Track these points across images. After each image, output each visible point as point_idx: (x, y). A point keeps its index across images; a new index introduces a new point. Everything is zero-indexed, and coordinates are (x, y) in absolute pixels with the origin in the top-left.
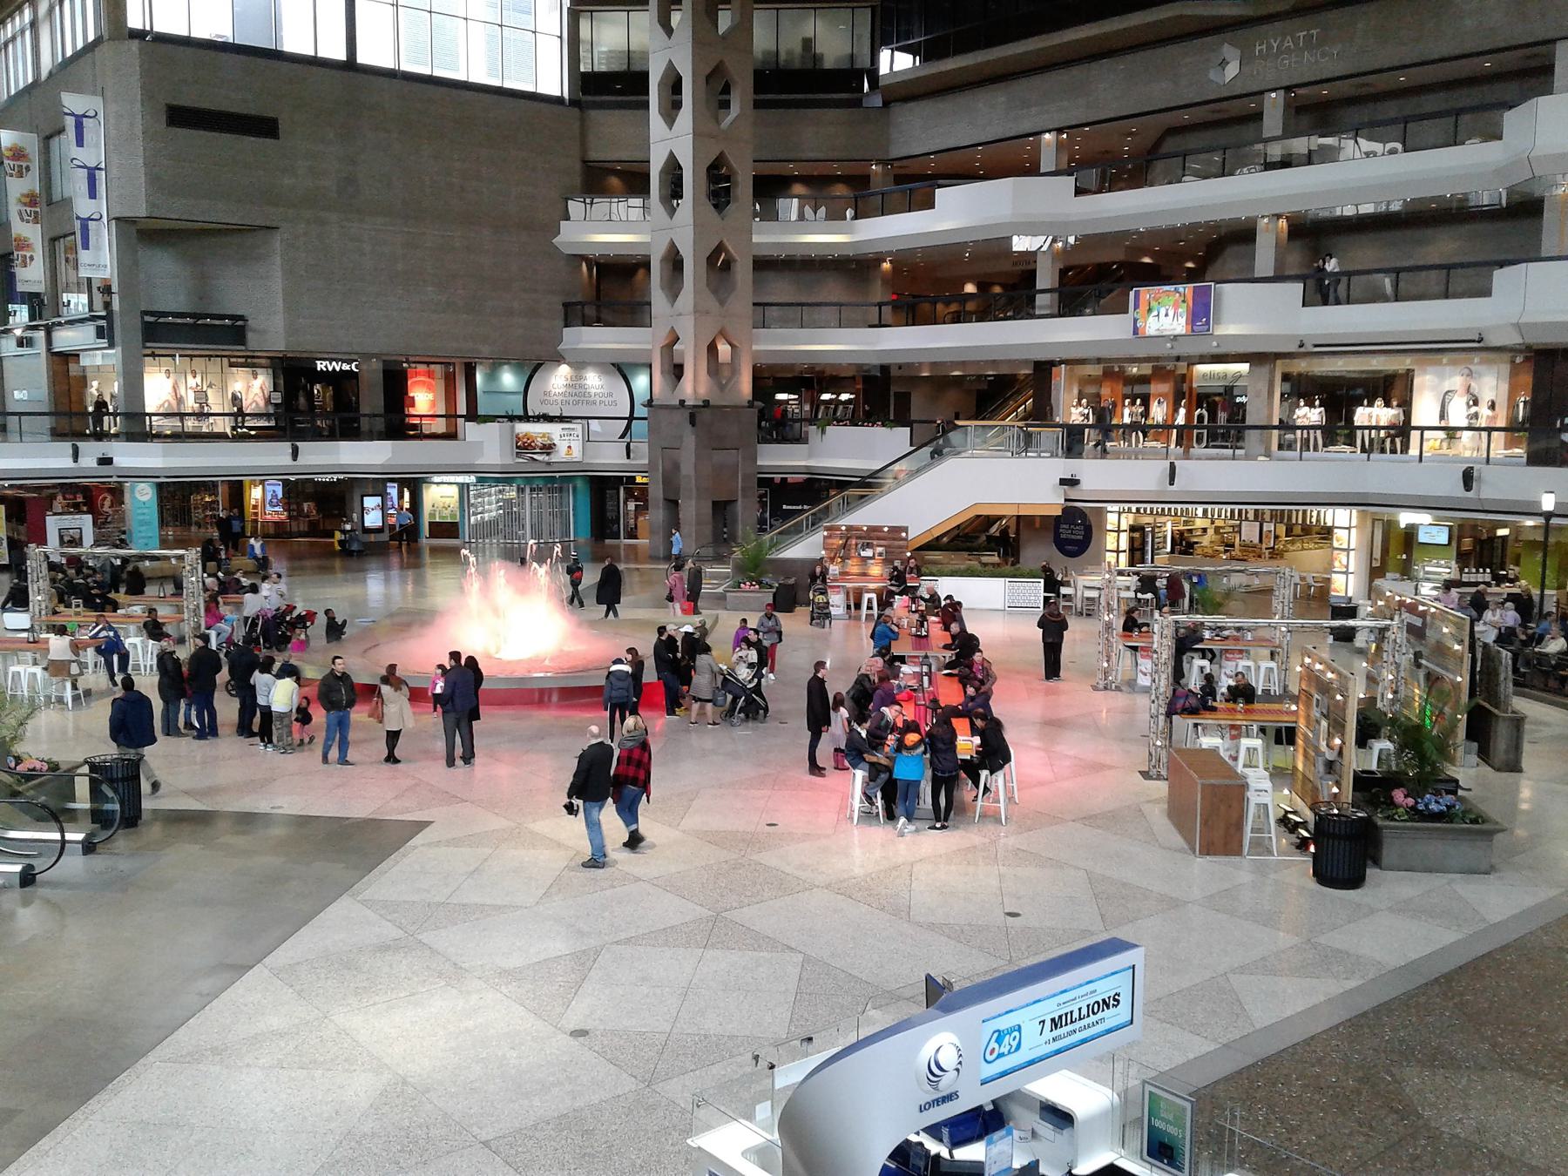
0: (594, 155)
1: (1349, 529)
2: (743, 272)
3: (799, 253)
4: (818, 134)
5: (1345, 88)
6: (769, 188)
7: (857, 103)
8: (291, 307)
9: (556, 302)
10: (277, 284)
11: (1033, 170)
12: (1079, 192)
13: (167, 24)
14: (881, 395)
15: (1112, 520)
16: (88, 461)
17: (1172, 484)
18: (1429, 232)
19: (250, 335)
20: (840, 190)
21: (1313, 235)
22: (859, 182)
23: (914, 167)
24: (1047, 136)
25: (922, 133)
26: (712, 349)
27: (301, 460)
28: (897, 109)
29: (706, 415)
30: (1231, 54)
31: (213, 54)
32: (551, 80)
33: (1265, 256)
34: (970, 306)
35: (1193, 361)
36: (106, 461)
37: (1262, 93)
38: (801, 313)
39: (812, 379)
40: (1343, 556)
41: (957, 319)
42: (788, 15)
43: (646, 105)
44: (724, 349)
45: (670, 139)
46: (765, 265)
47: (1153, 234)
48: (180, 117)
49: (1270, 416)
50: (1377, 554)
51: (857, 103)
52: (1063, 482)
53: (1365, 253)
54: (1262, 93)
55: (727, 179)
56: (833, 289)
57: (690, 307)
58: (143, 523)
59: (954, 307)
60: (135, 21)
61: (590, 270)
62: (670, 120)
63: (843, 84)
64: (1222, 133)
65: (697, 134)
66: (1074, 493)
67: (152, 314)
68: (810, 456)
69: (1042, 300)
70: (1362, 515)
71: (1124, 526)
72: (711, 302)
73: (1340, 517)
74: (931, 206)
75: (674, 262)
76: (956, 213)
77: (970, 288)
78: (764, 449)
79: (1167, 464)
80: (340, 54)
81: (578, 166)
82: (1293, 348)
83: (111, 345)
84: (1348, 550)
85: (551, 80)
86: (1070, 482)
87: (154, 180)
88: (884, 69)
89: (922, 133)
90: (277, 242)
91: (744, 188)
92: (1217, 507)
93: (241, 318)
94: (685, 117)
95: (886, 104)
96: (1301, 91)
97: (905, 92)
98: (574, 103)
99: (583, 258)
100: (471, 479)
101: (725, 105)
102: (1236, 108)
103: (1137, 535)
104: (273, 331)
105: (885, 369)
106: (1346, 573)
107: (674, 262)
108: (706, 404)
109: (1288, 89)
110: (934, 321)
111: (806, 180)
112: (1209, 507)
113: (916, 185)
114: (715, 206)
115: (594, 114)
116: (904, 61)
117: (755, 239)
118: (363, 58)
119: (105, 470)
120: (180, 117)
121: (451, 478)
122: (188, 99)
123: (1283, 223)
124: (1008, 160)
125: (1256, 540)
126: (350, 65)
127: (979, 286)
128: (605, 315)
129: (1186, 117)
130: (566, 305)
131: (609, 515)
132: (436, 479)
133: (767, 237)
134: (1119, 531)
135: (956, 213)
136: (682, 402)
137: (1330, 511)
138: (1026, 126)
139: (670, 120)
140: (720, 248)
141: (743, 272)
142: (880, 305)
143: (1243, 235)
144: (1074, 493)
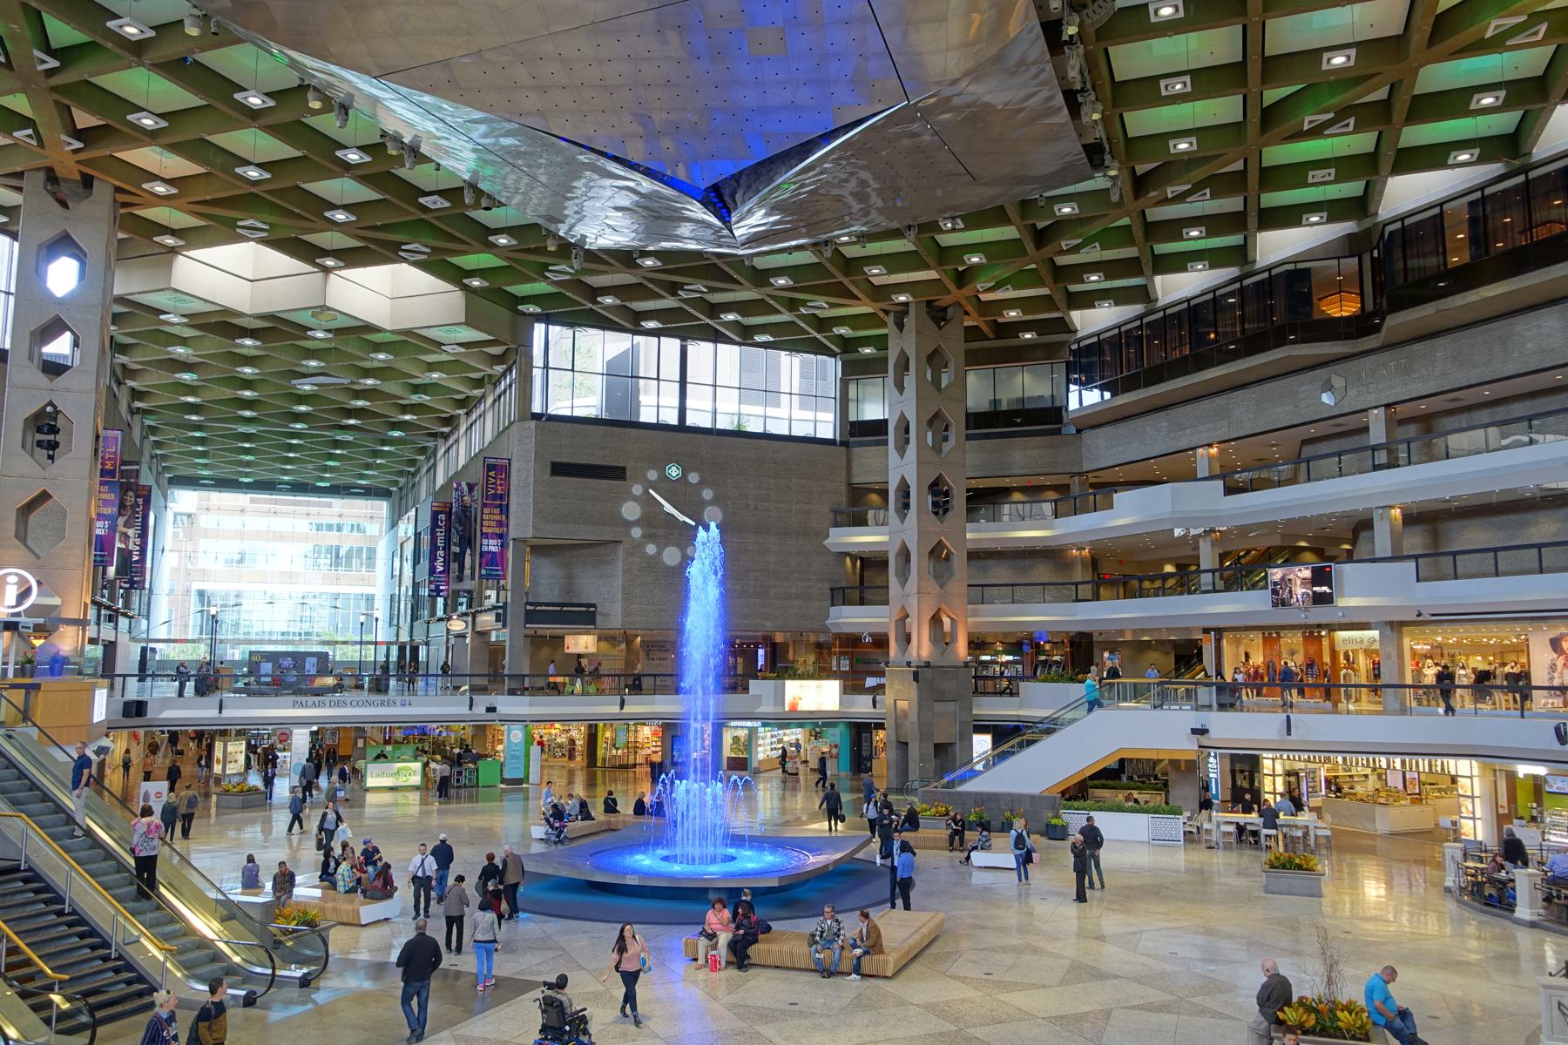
0: (855, 480)
1: (1471, 777)
2: (959, 562)
3: (1011, 545)
4: (1023, 456)
5: (1439, 404)
6: (985, 499)
7: (1058, 432)
8: (628, 599)
9: (827, 586)
10: (618, 582)
11: (1190, 476)
12: (1230, 490)
13: (560, 407)
14: (1080, 653)
15: (1267, 764)
16: (480, 710)
17: (1289, 733)
18: (1529, 516)
19: (598, 618)
20: (1052, 495)
21: (1429, 518)
22: (1063, 489)
23: (1106, 477)
24: (1200, 450)
26: (936, 620)
27: (627, 709)
28: (1086, 434)
29: (927, 673)
30: (1338, 382)
31: (590, 427)
32: (826, 427)
33: (1382, 540)
34: (1171, 582)
35: (1332, 628)
36: (491, 710)
37: (1366, 410)
38: (1016, 592)
40: (1468, 803)
41: (1162, 592)
42: (1003, 371)
43: (886, 443)
44: (946, 621)
45: (901, 466)
46: (975, 556)
47: (1303, 521)
48: (559, 469)
49: (1402, 674)
50: (1503, 800)
51: (1058, 432)
52: (1194, 731)
53: (1474, 535)
54: (1366, 410)
55: (947, 494)
56: (1042, 572)
57: (915, 590)
59: (1158, 584)
60: (537, 408)
61: (854, 564)
62: (901, 451)
63: (1048, 417)
64: (1336, 442)
65: (920, 462)
66: (1205, 741)
67: (531, 604)
68: (1021, 707)
69: (1206, 579)
70: (1483, 767)
71: (1279, 770)
72: (932, 586)
73: (1462, 767)
75: (905, 554)
76: (1128, 513)
77: (1169, 568)
78: (977, 700)
80: (674, 421)
81: (844, 488)
82: (1414, 618)
83: (504, 626)
84: (1472, 797)
85: (826, 427)
86: (1202, 732)
87: (538, 513)
88: (1073, 404)
89: (1103, 451)
90: (620, 552)
91: (959, 501)
92: (1354, 757)
93: (594, 605)
94: (912, 449)
95: (1079, 431)
96: (1399, 408)
97: (1094, 421)
98: (844, 444)
99: (847, 554)
100: (759, 723)
101: (946, 439)
102: (1351, 423)
103: (1292, 779)
104: (614, 614)
105: (1089, 636)
106: (1474, 818)
107: (905, 554)
108: (928, 665)
109: (1387, 406)
110: (1141, 594)
111: (1022, 489)
112: (1348, 756)
113: (1102, 489)
114: (936, 513)
115: (856, 450)
116: (1092, 397)
117: (969, 536)
118: (689, 422)
119: (491, 716)
120: (559, 469)
121: (740, 723)
122: (564, 459)
123: (1396, 513)
124: (1171, 469)
125: (1401, 787)
126: (682, 427)
127: (1177, 566)
128: (868, 595)
129: (1312, 431)
131: (864, 754)
132: (733, 723)
133: (979, 533)
134: (1274, 775)
135: (1128, 513)
137: (1452, 761)
138: (1183, 444)
139: (901, 451)
140: (939, 546)
141: (959, 562)
142: (1076, 584)
143: (1362, 525)
144: (1205, 741)
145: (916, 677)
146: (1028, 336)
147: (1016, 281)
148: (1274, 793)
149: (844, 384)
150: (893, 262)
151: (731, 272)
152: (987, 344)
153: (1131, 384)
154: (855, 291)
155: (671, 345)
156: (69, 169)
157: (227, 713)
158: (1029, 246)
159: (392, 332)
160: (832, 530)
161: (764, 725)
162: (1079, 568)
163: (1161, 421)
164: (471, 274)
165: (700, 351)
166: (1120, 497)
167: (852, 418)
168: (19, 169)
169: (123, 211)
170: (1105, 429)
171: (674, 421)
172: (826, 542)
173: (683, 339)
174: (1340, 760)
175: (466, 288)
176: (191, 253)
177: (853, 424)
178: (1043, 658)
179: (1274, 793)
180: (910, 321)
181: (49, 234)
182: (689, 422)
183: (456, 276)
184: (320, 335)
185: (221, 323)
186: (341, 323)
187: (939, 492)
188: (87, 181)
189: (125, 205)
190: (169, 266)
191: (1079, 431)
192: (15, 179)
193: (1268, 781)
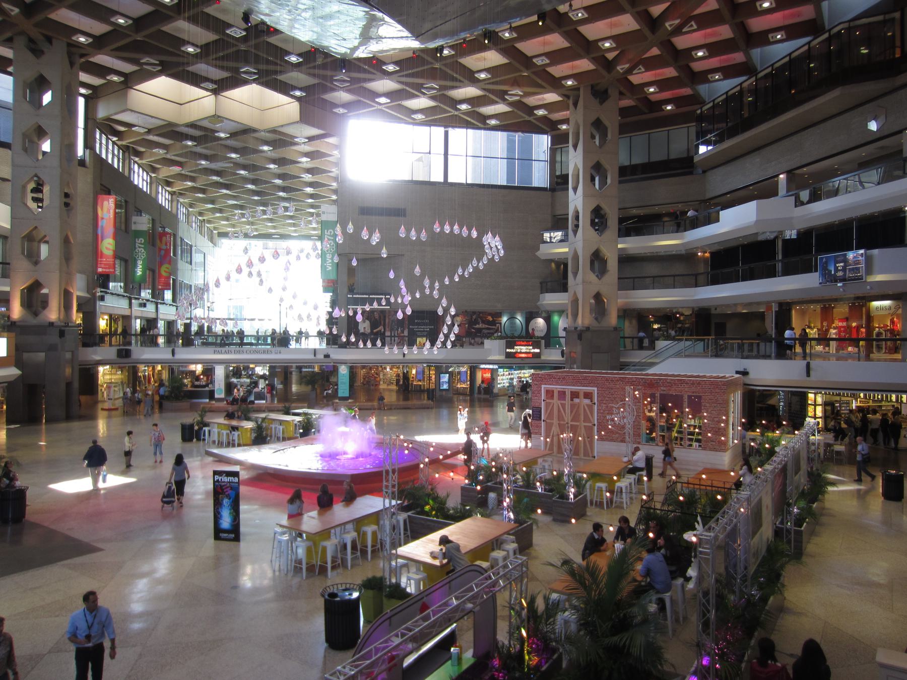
17: (808, 374)
24: (781, 176)
25: (721, 181)
28: (709, 174)
38: (657, 282)
39: (667, 317)
46: (626, 260)
51: (691, 173)
56: (679, 268)
58: (343, 383)
63: (685, 165)
65: (585, 196)
71: (819, 400)
74: (717, 220)
79: (805, 362)
86: (745, 373)
97: (713, 164)
99: (551, 261)
100: (496, 367)
108: (588, 329)
118: (450, 180)
119: (327, 360)
130: (541, 283)
132: (483, 366)
134: (815, 405)
136: (576, 328)
145: (580, 337)
146: (669, 108)
147: (650, 64)
148: (815, 417)
149: (553, 151)
150: (557, 57)
151: (449, 72)
152: (644, 117)
153: (732, 132)
154: (540, 81)
155: (440, 131)
156: (35, 33)
157: (177, 356)
158: (647, 32)
159: (264, 131)
160: (542, 246)
161: (500, 367)
162: (702, 265)
163: (756, 159)
164: (295, 88)
165: (458, 135)
166: (724, 214)
167: (558, 173)
168: (8, 35)
169: (83, 60)
170: (720, 169)
171: (442, 180)
172: (538, 253)
173: (445, 127)
174: (862, 395)
175: (298, 99)
176: (137, 87)
177: (558, 177)
178: (679, 325)
179: (815, 417)
180: (581, 103)
181: (30, 75)
182: (450, 180)
183: (284, 88)
184: (222, 135)
185: (172, 132)
186: (233, 127)
187: (598, 219)
188: (49, 40)
189: (82, 56)
190: (125, 96)
191: (704, 172)
192: (9, 42)
193: (810, 409)
